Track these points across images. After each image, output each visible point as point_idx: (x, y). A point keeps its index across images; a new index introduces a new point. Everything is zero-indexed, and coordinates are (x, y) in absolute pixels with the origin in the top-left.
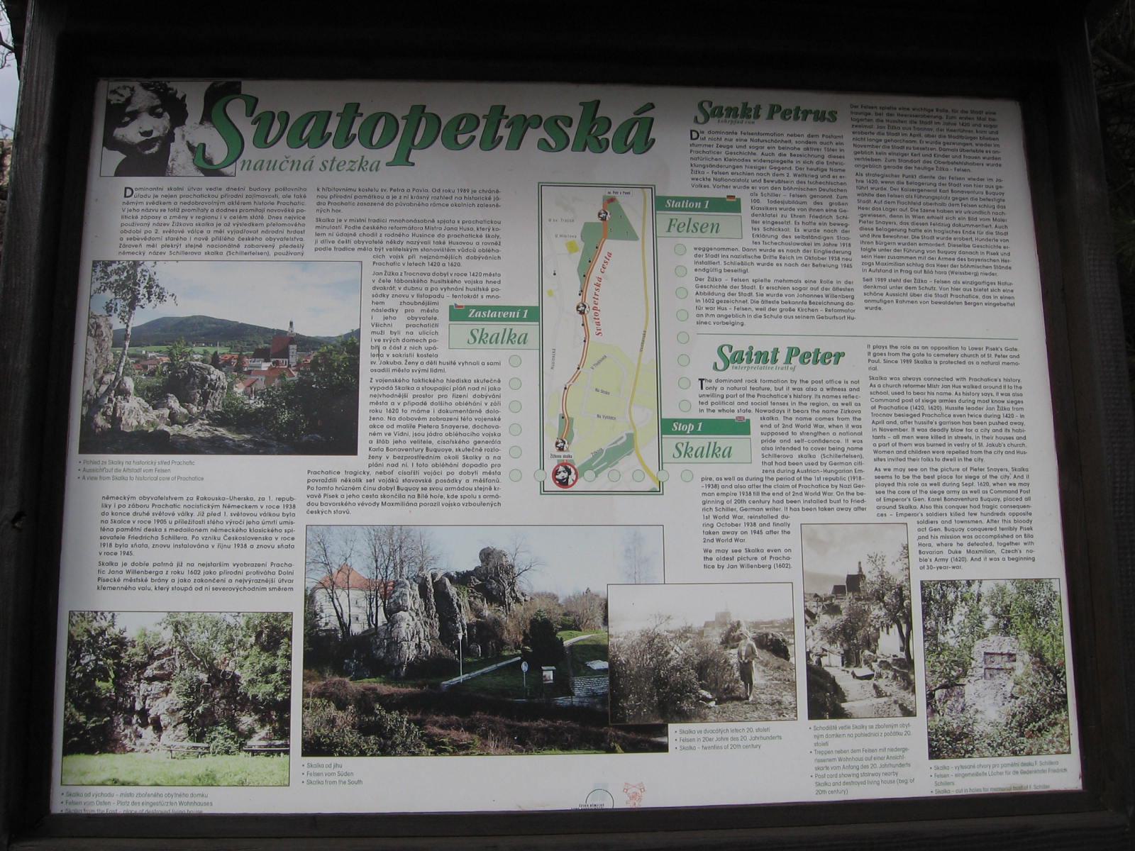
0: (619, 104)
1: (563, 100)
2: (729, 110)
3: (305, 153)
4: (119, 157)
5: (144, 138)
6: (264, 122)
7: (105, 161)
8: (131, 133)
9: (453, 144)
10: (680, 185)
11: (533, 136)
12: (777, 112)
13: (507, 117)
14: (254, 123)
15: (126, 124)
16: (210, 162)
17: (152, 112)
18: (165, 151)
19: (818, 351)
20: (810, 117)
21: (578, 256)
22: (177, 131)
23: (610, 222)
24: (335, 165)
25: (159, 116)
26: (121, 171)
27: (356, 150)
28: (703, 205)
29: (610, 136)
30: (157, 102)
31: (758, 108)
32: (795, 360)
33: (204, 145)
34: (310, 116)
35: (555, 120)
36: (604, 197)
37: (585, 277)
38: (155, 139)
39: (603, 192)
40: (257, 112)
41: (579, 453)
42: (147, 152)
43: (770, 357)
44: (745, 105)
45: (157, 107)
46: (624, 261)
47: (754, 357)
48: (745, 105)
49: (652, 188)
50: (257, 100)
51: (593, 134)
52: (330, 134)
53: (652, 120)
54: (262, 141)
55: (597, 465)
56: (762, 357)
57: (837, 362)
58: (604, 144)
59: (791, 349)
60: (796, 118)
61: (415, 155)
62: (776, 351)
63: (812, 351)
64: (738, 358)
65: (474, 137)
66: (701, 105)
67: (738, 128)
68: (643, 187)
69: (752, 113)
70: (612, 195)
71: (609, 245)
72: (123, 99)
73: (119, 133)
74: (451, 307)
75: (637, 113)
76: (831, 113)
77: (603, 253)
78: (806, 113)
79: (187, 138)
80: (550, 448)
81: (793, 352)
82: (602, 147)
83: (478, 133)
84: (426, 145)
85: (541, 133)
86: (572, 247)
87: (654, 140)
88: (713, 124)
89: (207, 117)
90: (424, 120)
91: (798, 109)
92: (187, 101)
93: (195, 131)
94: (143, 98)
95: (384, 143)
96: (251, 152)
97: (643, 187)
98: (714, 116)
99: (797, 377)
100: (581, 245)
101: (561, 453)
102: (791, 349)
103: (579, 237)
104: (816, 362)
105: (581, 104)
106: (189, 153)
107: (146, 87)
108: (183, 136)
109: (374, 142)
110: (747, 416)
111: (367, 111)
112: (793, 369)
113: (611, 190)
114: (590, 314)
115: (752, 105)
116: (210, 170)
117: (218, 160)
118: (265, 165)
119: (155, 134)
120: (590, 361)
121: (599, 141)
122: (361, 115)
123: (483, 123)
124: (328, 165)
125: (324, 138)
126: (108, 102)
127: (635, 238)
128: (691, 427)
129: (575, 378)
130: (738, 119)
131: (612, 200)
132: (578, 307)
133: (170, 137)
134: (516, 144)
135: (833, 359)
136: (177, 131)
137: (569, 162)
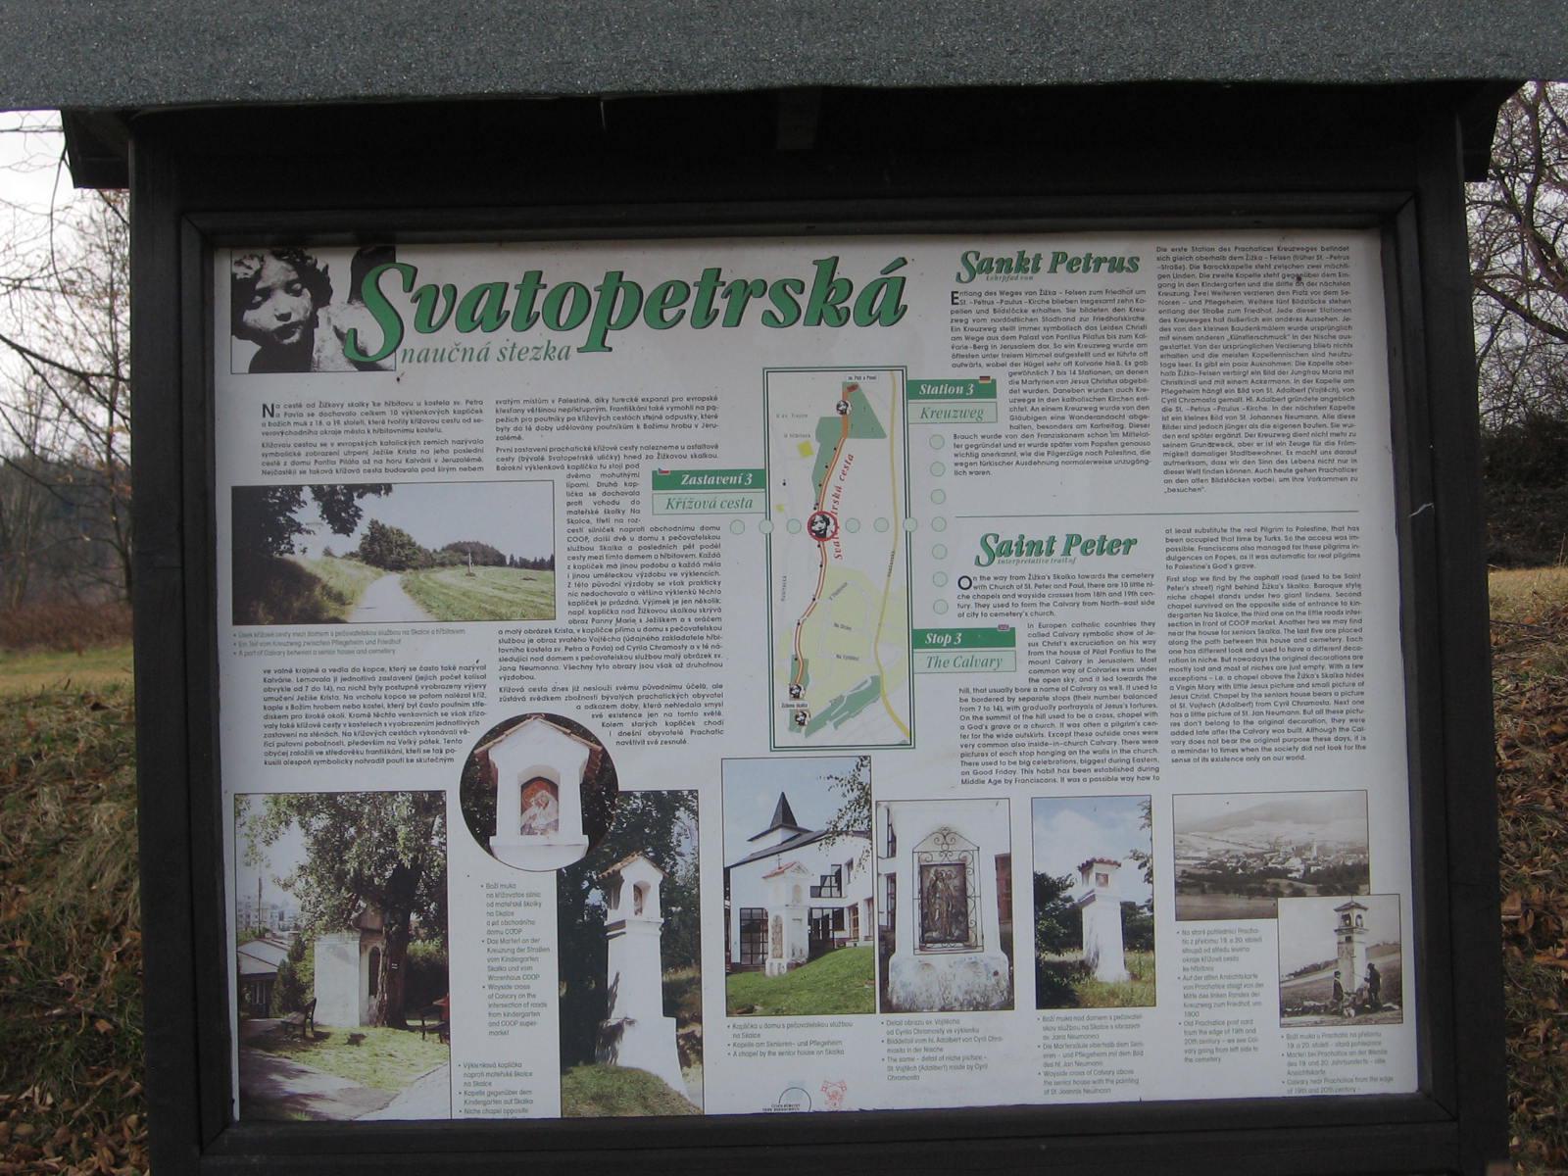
0: (861, 262)
1: (791, 261)
2: (1002, 262)
3: (477, 338)
5: (281, 324)
6: (426, 298)
8: (263, 317)
9: (659, 322)
10: (936, 365)
11: (757, 306)
12: (1063, 261)
13: (724, 284)
14: (414, 300)
15: (257, 306)
16: (363, 352)
17: (288, 288)
19: (1104, 538)
20: (1105, 266)
21: (812, 461)
22: (320, 312)
23: (851, 416)
24: (513, 354)
25: (298, 293)
26: (259, 366)
27: (540, 333)
28: (966, 390)
29: (850, 303)
30: (293, 276)
31: (1038, 257)
32: (1075, 551)
33: (355, 331)
34: (482, 290)
35: (783, 284)
36: (844, 384)
38: (295, 325)
40: (419, 284)
42: (286, 341)
43: (1044, 548)
44: (1021, 254)
45: (294, 282)
47: (1025, 548)
48: (1021, 254)
49: (903, 369)
50: (416, 270)
51: (831, 303)
52: (508, 312)
53: (904, 279)
54: (426, 325)
55: (836, 715)
56: (1035, 548)
57: (1126, 552)
58: (843, 314)
59: (1070, 537)
60: (1086, 269)
61: (612, 338)
62: (1052, 540)
63: (1097, 538)
64: (1005, 549)
66: (965, 258)
68: (891, 369)
69: (1030, 266)
70: (854, 381)
71: (850, 445)
72: (251, 273)
73: (250, 317)
74: (654, 473)
75: (884, 272)
76: (1131, 260)
78: (1099, 261)
79: (334, 321)
80: (782, 694)
81: (1072, 540)
82: (841, 319)
83: (689, 306)
84: (626, 323)
87: (906, 307)
88: (981, 282)
89: (356, 294)
90: (621, 290)
91: (1089, 256)
92: (330, 274)
93: (342, 312)
94: (276, 270)
95: (572, 325)
96: (412, 339)
97: (891, 369)
98: (981, 270)
99: (1073, 570)
100: (816, 446)
101: (795, 702)
102: (1070, 537)
103: (813, 435)
104: (1101, 551)
105: (815, 262)
106: (338, 342)
108: (329, 319)
109: (562, 322)
110: (1010, 621)
111: (551, 280)
112: (1073, 562)
115: (1030, 254)
116: (365, 364)
118: (431, 355)
119: (294, 318)
120: (829, 587)
121: (837, 311)
122: (545, 286)
123: (694, 291)
124: (507, 354)
125: (501, 318)
126: (234, 276)
128: (948, 638)
129: (809, 612)
130: (1013, 274)
131: (853, 388)
133: (312, 322)
134: (735, 319)
135: (1122, 548)
136: (320, 312)
137: (803, 340)
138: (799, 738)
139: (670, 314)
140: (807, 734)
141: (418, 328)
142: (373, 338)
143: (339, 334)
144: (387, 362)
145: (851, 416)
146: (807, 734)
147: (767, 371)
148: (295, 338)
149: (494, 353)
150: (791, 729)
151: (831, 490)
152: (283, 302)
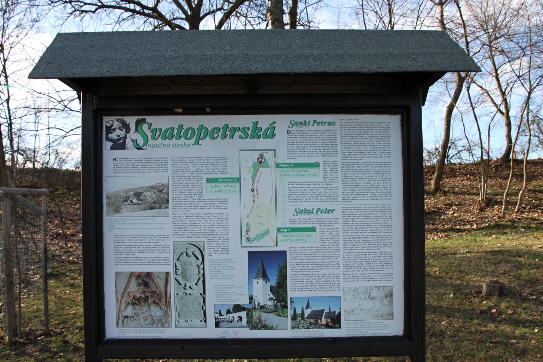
2: (300, 123)
4: (110, 144)
7: (107, 145)
9: (213, 138)
11: (238, 134)
15: (112, 133)
16: (138, 145)
17: (120, 129)
18: (124, 142)
20: (327, 124)
21: (251, 173)
22: (128, 135)
25: (122, 130)
26: (112, 148)
27: (183, 140)
29: (261, 133)
30: (121, 125)
37: (253, 180)
39: (260, 152)
41: (252, 235)
48: (305, 121)
54: (154, 138)
60: (322, 125)
65: (219, 135)
67: (302, 129)
71: (261, 170)
72: (110, 125)
73: (110, 136)
75: (270, 125)
76: (333, 122)
77: (259, 173)
78: (325, 123)
82: (259, 137)
83: (220, 134)
85: (240, 133)
86: (249, 171)
92: (130, 125)
96: (151, 142)
100: (252, 170)
107: (117, 120)
114: (255, 192)
115: (307, 121)
117: (141, 145)
120: (255, 207)
123: (221, 130)
125: (173, 136)
127: (269, 167)
129: (250, 212)
131: (262, 155)
133: (126, 137)
136: (128, 135)
137: (249, 143)
139: (215, 136)
141: (152, 139)
142: (141, 142)
143: (133, 141)
144: (144, 148)
147: (240, 151)
148: (121, 141)
149: (171, 146)
151: (256, 181)
152: (118, 132)
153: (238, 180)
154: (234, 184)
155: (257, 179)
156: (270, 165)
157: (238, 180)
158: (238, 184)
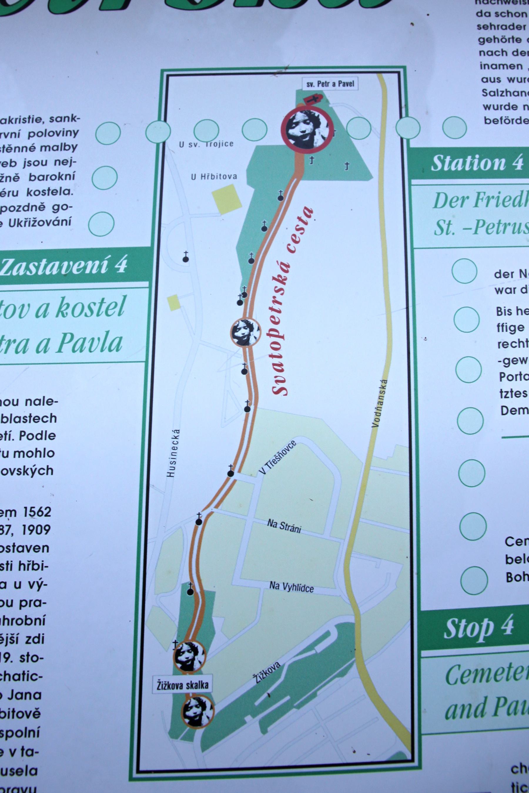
21: (237, 218)
36: (299, 92)
37: (252, 262)
39: (300, 83)
46: (343, 219)
55: (264, 706)
68: (379, 71)
70: (316, 88)
71: (307, 192)
86: (226, 201)
97: (379, 71)
100: (246, 193)
101: (186, 678)
103: (243, 177)
113: (314, 79)
114: (261, 347)
127: (366, 176)
132: (235, 329)
138: (188, 752)
140: (205, 745)
145: (308, 136)
146: (205, 745)
150: (174, 734)
151: (270, 269)
153: (141, 264)
154: (112, 292)
155: (277, 251)
156: (371, 162)
157: (141, 264)
158: (137, 293)
